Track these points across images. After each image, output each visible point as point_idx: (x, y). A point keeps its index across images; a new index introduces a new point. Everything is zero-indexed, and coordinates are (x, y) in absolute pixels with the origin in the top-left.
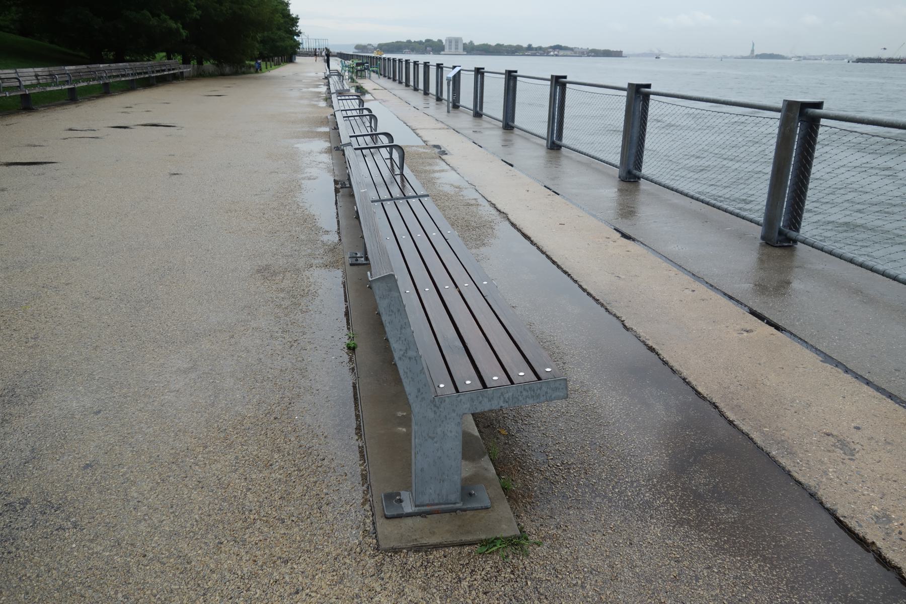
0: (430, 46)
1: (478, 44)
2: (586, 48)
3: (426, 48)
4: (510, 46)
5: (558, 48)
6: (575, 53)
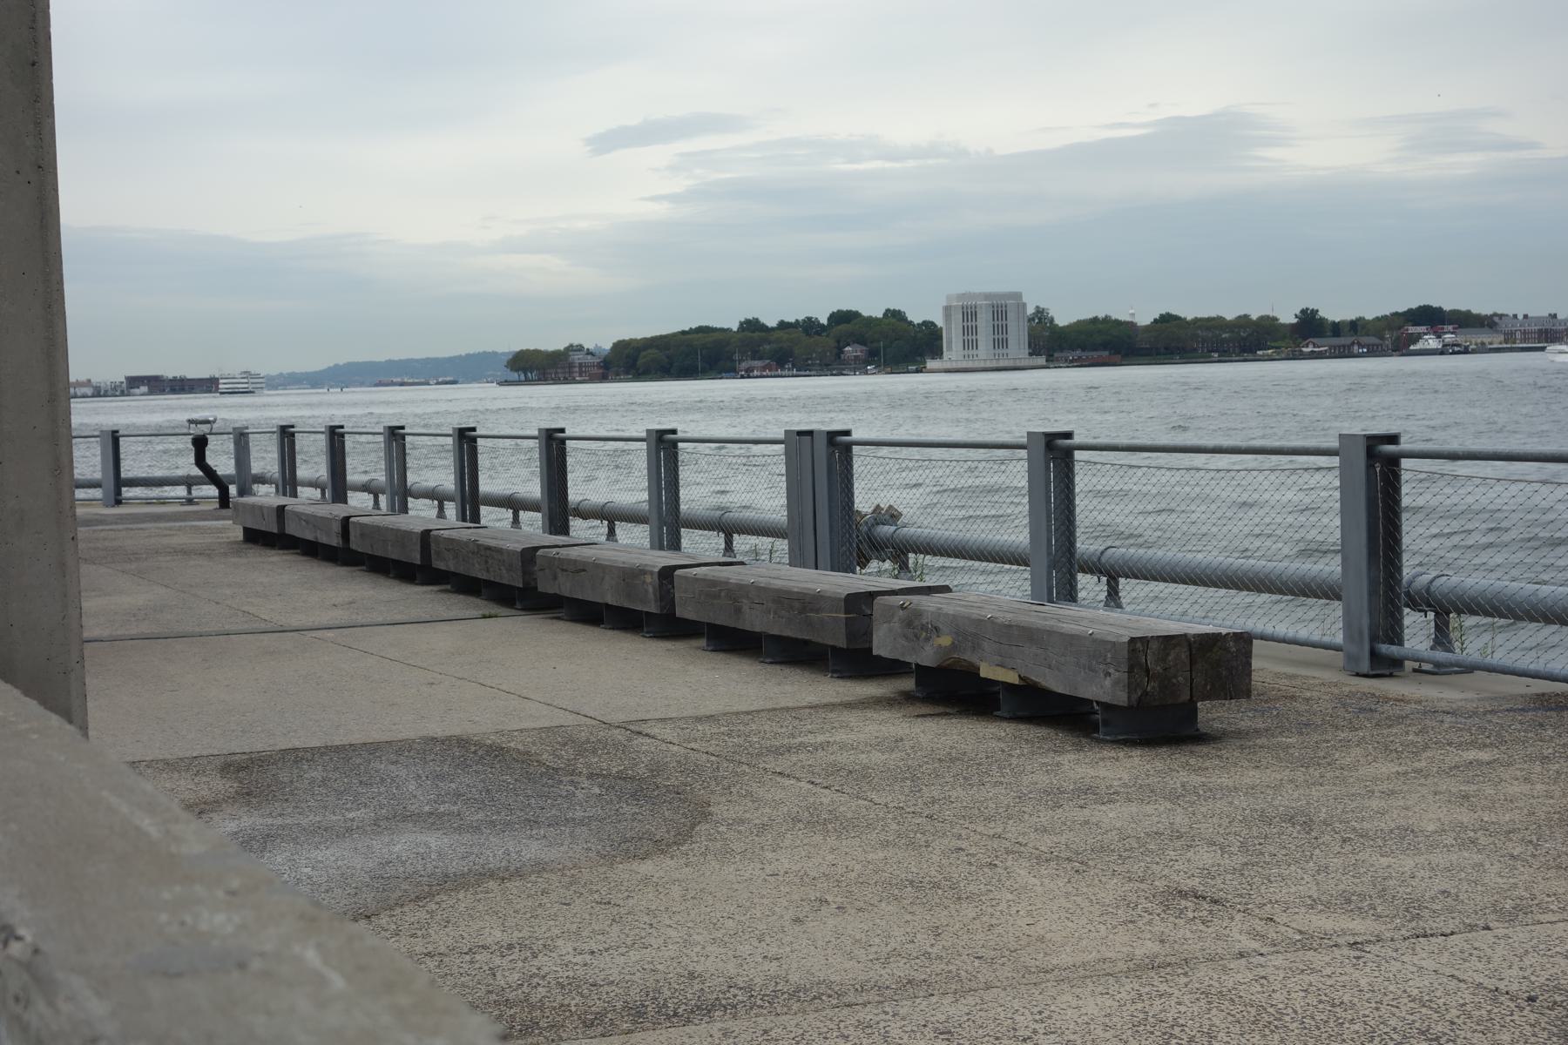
0: (860, 340)
1: (1066, 324)
2: (1544, 312)
3: (840, 351)
4: (1213, 325)
5: (1430, 317)
6: (1509, 336)
